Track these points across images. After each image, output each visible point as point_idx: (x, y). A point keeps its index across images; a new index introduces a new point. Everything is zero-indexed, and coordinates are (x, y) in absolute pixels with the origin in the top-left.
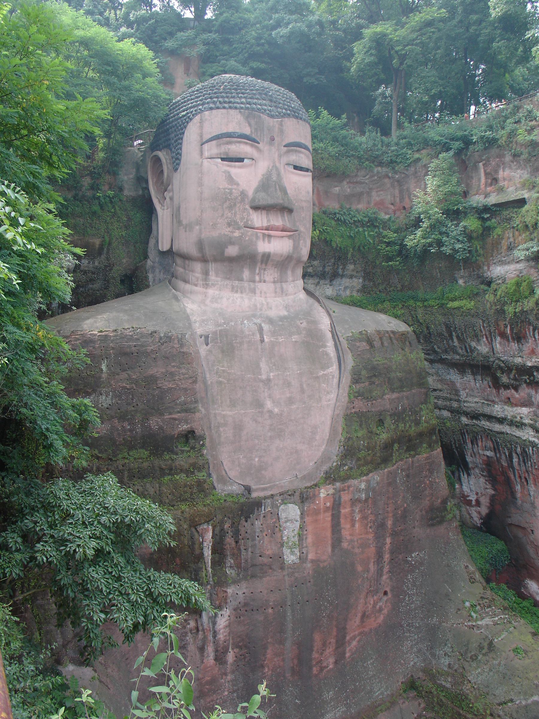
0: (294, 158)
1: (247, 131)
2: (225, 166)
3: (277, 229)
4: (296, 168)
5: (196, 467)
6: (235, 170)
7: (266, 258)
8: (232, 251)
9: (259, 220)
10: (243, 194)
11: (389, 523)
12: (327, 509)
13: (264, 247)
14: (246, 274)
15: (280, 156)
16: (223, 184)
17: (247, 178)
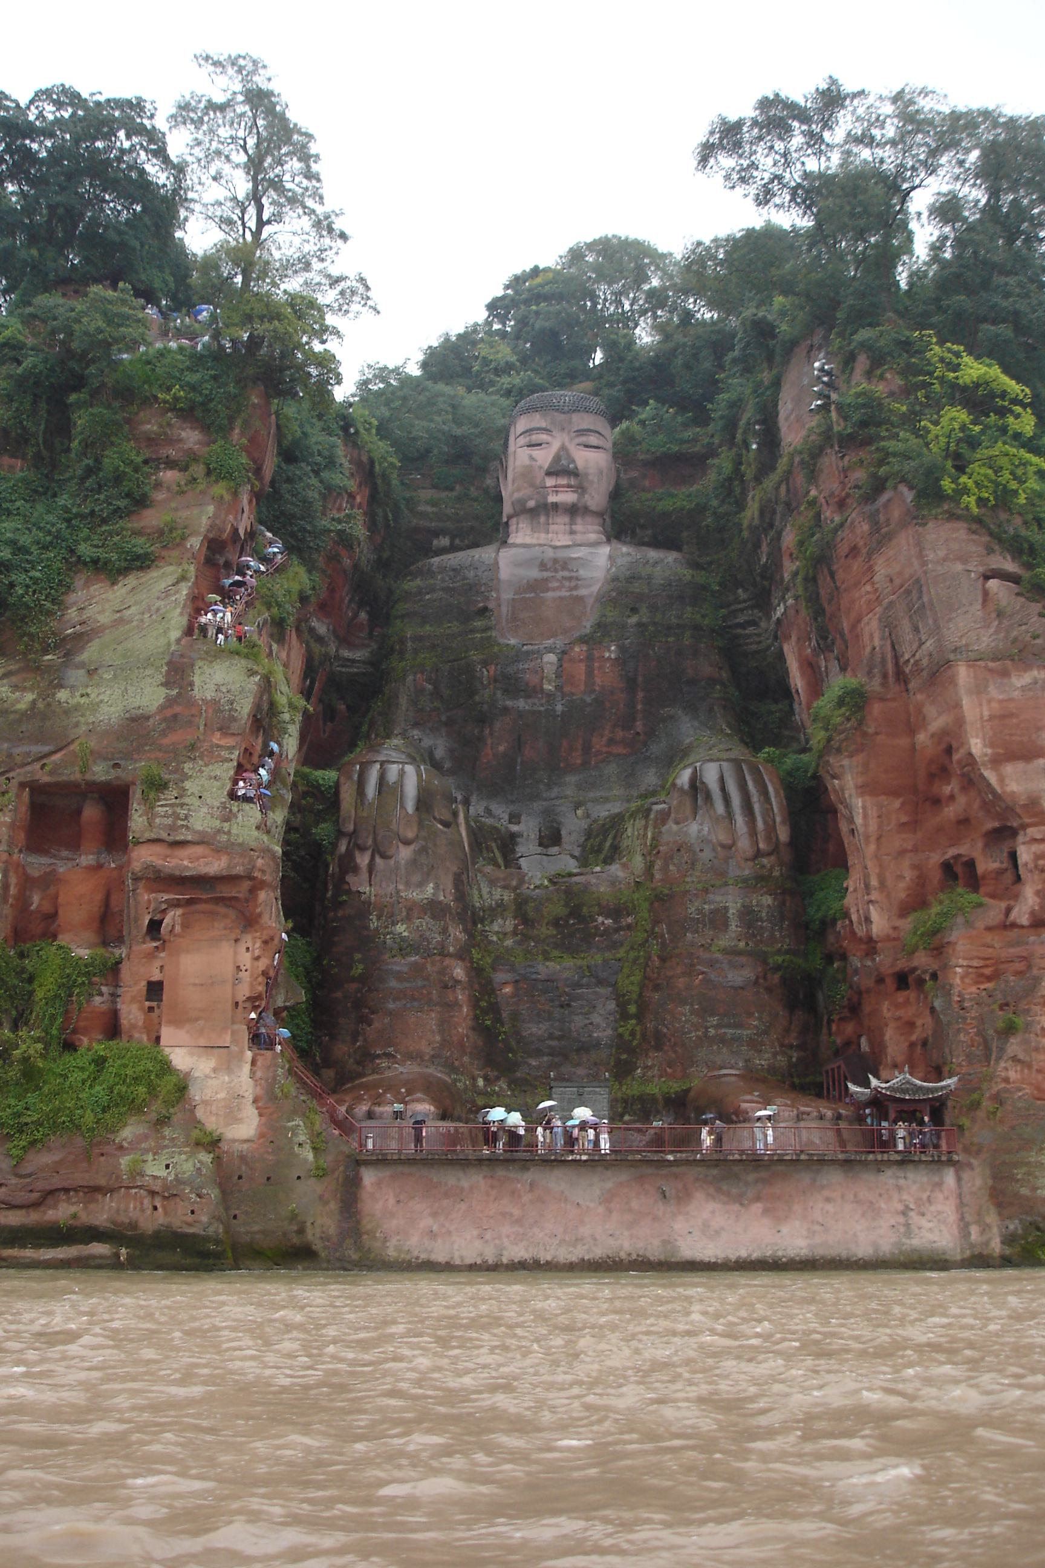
0: (583, 439)
1: (544, 425)
2: (527, 451)
3: (563, 486)
4: (586, 446)
5: (488, 628)
6: (536, 453)
7: (555, 506)
8: (531, 504)
9: (550, 482)
10: (540, 467)
11: (640, 679)
12: (581, 661)
13: (552, 499)
14: (542, 519)
15: (571, 440)
16: (527, 462)
17: (544, 457)
